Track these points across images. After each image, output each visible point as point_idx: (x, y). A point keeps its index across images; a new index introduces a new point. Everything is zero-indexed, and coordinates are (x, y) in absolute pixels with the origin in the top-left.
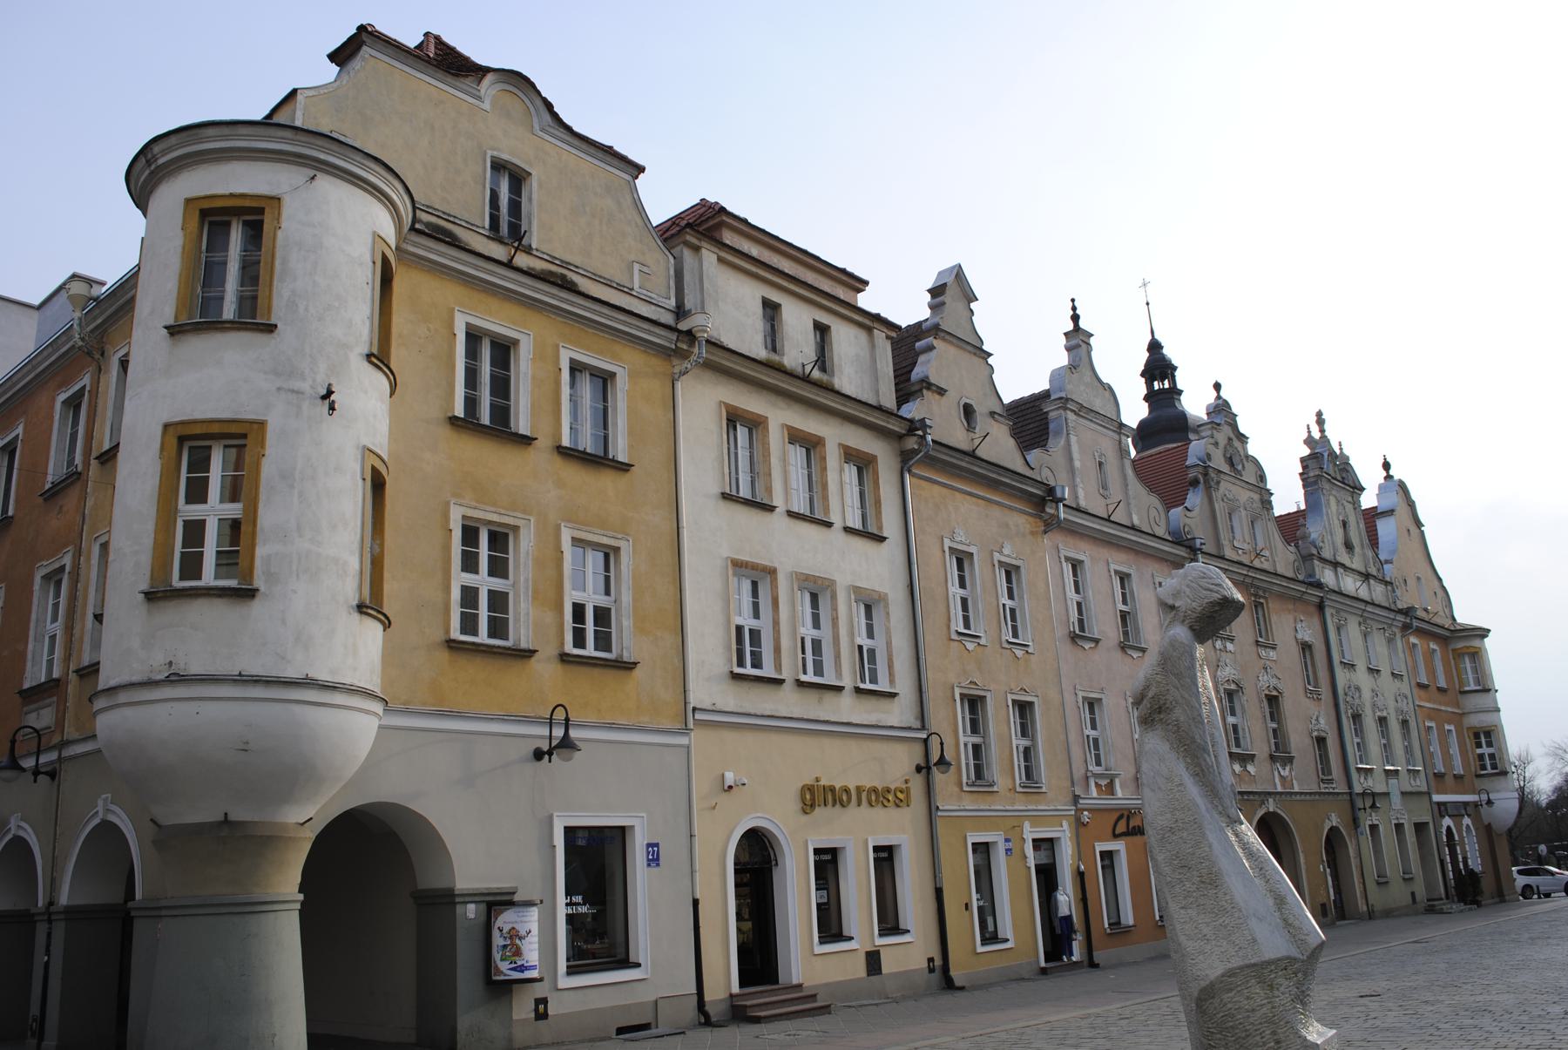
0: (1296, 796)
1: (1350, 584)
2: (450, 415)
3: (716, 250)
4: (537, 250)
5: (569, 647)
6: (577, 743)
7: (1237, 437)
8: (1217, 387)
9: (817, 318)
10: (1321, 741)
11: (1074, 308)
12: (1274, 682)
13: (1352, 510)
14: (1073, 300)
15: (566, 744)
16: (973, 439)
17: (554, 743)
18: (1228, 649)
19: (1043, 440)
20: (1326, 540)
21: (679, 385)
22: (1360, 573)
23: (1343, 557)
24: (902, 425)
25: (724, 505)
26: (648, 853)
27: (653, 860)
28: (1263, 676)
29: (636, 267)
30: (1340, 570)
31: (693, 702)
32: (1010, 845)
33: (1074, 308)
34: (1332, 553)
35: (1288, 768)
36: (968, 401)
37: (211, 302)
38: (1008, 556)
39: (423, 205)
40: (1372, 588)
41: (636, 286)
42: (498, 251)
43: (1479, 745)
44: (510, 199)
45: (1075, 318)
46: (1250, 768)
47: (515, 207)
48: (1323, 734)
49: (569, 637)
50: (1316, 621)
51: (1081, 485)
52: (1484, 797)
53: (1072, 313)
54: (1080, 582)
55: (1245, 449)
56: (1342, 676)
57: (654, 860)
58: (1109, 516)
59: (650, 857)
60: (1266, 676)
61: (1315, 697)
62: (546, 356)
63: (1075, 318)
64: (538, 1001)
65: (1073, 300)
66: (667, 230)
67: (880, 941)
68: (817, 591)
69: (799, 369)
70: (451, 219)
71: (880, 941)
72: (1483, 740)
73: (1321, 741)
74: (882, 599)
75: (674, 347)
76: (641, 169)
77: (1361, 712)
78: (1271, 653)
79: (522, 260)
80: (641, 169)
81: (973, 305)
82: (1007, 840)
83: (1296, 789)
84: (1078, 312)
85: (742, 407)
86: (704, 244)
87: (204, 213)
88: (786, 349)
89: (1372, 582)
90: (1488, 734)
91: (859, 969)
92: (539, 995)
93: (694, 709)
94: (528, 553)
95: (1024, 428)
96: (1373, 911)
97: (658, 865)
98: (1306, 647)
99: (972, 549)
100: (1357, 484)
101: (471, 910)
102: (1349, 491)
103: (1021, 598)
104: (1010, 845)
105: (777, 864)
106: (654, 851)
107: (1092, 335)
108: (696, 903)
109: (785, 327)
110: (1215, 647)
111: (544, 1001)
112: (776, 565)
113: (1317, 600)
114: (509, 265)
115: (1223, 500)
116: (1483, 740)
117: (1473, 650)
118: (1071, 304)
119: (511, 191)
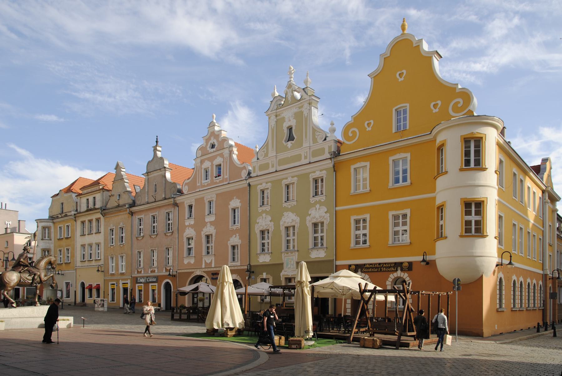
32: (117, 284)
38: (121, 225)
57: (71, 286)
67: (96, 299)
68: (91, 245)
71: (96, 299)
74: (100, 243)
79: (63, 215)
82: (117, 283)
84: (158, 140)
91: (93, 302)
99: (114, 227)
103: (138, 229)
104: (117, 284)
108: (75, 291)
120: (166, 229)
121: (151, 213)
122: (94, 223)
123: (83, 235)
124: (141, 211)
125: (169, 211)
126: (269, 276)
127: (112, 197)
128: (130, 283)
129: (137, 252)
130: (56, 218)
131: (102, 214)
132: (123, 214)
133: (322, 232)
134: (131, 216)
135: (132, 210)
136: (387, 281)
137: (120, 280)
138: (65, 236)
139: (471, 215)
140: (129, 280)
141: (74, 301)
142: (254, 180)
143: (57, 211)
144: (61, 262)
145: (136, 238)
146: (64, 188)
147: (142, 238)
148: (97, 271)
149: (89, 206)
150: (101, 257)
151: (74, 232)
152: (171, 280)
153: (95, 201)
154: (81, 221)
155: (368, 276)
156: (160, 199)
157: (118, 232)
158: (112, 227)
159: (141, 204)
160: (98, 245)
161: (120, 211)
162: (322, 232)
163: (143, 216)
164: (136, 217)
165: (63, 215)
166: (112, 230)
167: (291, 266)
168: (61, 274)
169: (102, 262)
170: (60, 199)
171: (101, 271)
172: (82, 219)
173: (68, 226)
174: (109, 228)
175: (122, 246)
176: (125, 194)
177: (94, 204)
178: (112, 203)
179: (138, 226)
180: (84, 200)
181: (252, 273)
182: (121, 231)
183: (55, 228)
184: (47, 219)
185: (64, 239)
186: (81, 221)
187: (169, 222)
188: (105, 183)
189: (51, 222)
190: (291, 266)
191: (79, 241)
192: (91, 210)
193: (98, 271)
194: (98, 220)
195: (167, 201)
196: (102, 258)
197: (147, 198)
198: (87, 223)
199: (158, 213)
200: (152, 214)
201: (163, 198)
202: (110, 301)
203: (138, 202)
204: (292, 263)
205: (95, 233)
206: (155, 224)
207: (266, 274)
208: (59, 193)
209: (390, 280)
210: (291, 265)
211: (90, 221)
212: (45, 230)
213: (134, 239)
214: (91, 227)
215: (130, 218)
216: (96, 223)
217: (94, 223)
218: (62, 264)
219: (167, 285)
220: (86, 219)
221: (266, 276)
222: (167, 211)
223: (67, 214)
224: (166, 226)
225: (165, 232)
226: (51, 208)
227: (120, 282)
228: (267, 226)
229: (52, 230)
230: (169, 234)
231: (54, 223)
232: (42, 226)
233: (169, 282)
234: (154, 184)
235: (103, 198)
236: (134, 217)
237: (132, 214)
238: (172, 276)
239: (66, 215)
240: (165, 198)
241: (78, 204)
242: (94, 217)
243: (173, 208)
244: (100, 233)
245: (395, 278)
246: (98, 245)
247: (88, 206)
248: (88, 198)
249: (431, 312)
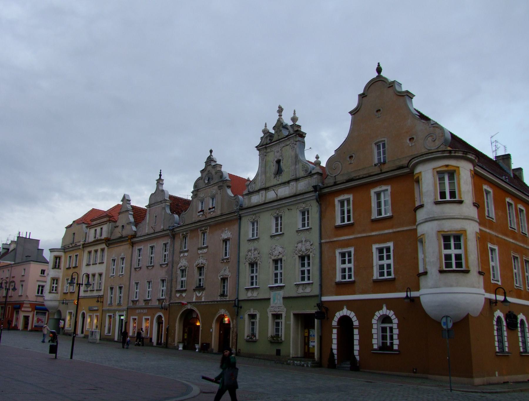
0: (203, 303)
8: (211, 151)
11: (161, 173)
14: (161, 170)
19: (141, 221)
25: (87, 266)
33: (161, 173)
35: (201, 293)
37: (56, 266)
43: (447, 247)
45: (160, 175)
46: (184, 295)
53: (160, 174)
58: (154, 231)
63: (160, 175)
65: (161, 170)
72: (452, 243)
79: (73, 245)
82: (113, 315)
83: (203, 300)
87: (55, 257)
90: (457, 238)
96: (239, 352)
99: (116, 258)
102: (287, 139)
104: (114, 316)
114: (72, 247)
116: (452, 243)
117: (452, 169)
120: (162, 260)
121: (149, 245)
122: (99, 253)
123: (88, 265)
124: (141, 241)
125: (166, 242)
126: (256, 312)
127: (116, 229)
128: (125, 315)
129: (134, 283)
130: (67, 248)
131: (106, 245)
132: (125, 245)
133: (309, 265)
134: (131, 246)
135: (133, 240)
136: (373, 319)
137: (116, 312)
138: (73, 265)
140: (125, 312)
142: (249, 211)
143: (69, 241)
144: (67, 291)
145: (134, 269)
146: (78, 219)
147: (139, 269)
148: (97, 301)
149: (96, 236)
150: (101, 288)
151: (81, 261)
152: (163, 314)
153: (102, 232)
154: (88, 251)
155: (349, 311)
156: (159, 230)
157: (119, 263)
158: (114, 256)
159: (142, 235)
160: (100, 275)
161: (122, 241)
162: (309, 265)
163: (142, 247)
164: (137, 248)
165: (73, 245)
166: (114, 260)
167: (277, 301)
168: (65, 303)
169: (101, 293)
170: (73, 230)
171: (101, 302)
172: (89, 249)
173: (77, 256)
174: (112, 259)
175: (121, 276)
176: (128, 225)
177: (101, 235)
178: (118, 233)
179: (137, 257)
180: (92, 231)
181: (239, 308)
182: (122, 262)
183: (66, 257)
184: (60, 249)
185: (72, 268)
186: (88, 251)
187: (165, 253)
188: (113, 214)
189: (62, 252)
190: (277, 301)
191: (85, 270)
192: (97, 240)
193: (98, 301)
194: (103, 250)
196: (103, 288)
197: (147, 229)
198: (93, 252)
199: (156, 244)
200: (151, 245)
201: (162, 229)
202: (106, 333)
203: (139, 234)
204: (279, 298)
205: (99, 263)
206: (153, 255)
207: (254, 310)
208: (72, 224)
209: (376, 318)
210: (278, 301)
211: (96, 251)
212: (56, 260)
213: (133, 269)
214: (96, 256)
215: (131, 249)
216: (100, 253)
217: (99, 253)
218: (67, 293)
219: (160, 317)
220: (92, 249)
221: (253, 312)
222: (164, 242)
223: (77, 244)
224: (162, 257)
225: (161, 264)
226: (64, 239)
227: (116, 314)
228: (256, 259)
229: (63, 260)
230: (164, 266)
231: (65, 252)
232: (54, 255)
233: (161, 315)
234: (155, 215)
235: (109, 229)
236: (134, 247)
237: (133, 244)
238: (165, 309)
239: (76, 245)
240: (163, 229)
241: (87, 234)
242: (99, 247)
243: (170, 240)
244: (103, 263)
245: (381, 316)
246: (100, 275)
247: (96, 236)
248: (96, 229)
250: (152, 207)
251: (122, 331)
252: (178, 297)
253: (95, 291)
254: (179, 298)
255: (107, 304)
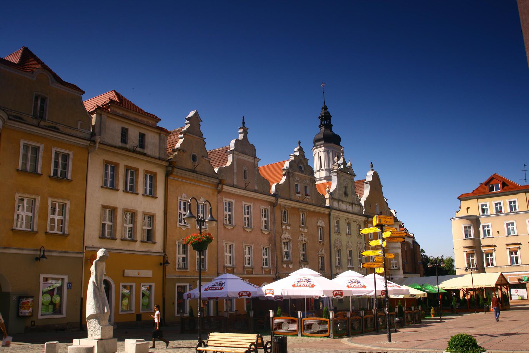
1: (344, 207)
2: (17, 169)
3: (106, 114)
4: (47, 120)
5: (48, 230)
6: (47, 257)
7: (304, 159)
9: (141, 132)
10: (322, 258)
11: (244, 120)
12: (306, 239)
13: (350, 182)
14: (243, 117)
15: (44, 256)
16: (194, 165)
17: (41, 256)
18: (287, 229)
20: (336, 193)
21: (90, 155)
22: (350, 203)
23: (344, 199)
24: (167, 163)
26: (68, 285)
27: (69, 287)
28: (301, 237)
29: (79, 122)
30: (340, 203)
31: (85, 245)
33: (244, 120)
34: (338, 196)
36: (194, 154)
39: (13, 111)
40: (353, 208)
41: (79, 128)
42: (35, 122)
44: (40, 105)
45: (244, 123)
47: (42, 108)
48: (323, 256)
49: (48, 228)
50: (327, 219)
51: (236, 178)
52: (391, 277)
54: (231, 209)
55: (307, 163)
56: (334, 237)
59: (69, 286)
60: (302, 237)
61: (322, 244)
62: (48, 151)
63: (244, 123)
64: (32, 322)
65: (243, 117)
66: (92, 109)
69: (132, 148)
70: (21, 114)
73: (322, 258)
75: (89, 145)
76: (84, 92)
77: (341, 249)
78: (305, 230)
79: (42, 123)
80: (84, 92)
81: (200, 123)
82: (190, 285)
85: (111, 161)
86: (103, 113)
88: (129, 142)
89: (354, 206)
92: (33, 320)
93: (86, 247)
94: (38, 206)
95: (222, 158)
97: (71, 288)
98: (321, 228)
100: (353, 174)
101: (14, 298)
105: (110, 289)
106: (70, 285)
107: (248, 129)
109: (129, 136)
110: (282, 228)
111: (34, 322)
112: (118, 206)
113: (328, 213)
114: (38, 126)
115: (294, 180)
118: (243, 118)
119: (41, 103)
132: (205, 187)
139: (393, 260)
141: (79, 320)
163: (233, 201)
195: (266, 197)
249: (406, 301)
250: (240, 156)
251: (104, 311)
252: (285, 268)
253: (118, 241)
254: (286, 269)
255: (175, 269)
